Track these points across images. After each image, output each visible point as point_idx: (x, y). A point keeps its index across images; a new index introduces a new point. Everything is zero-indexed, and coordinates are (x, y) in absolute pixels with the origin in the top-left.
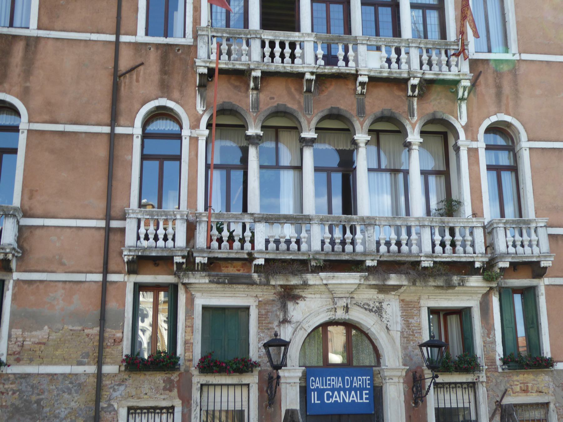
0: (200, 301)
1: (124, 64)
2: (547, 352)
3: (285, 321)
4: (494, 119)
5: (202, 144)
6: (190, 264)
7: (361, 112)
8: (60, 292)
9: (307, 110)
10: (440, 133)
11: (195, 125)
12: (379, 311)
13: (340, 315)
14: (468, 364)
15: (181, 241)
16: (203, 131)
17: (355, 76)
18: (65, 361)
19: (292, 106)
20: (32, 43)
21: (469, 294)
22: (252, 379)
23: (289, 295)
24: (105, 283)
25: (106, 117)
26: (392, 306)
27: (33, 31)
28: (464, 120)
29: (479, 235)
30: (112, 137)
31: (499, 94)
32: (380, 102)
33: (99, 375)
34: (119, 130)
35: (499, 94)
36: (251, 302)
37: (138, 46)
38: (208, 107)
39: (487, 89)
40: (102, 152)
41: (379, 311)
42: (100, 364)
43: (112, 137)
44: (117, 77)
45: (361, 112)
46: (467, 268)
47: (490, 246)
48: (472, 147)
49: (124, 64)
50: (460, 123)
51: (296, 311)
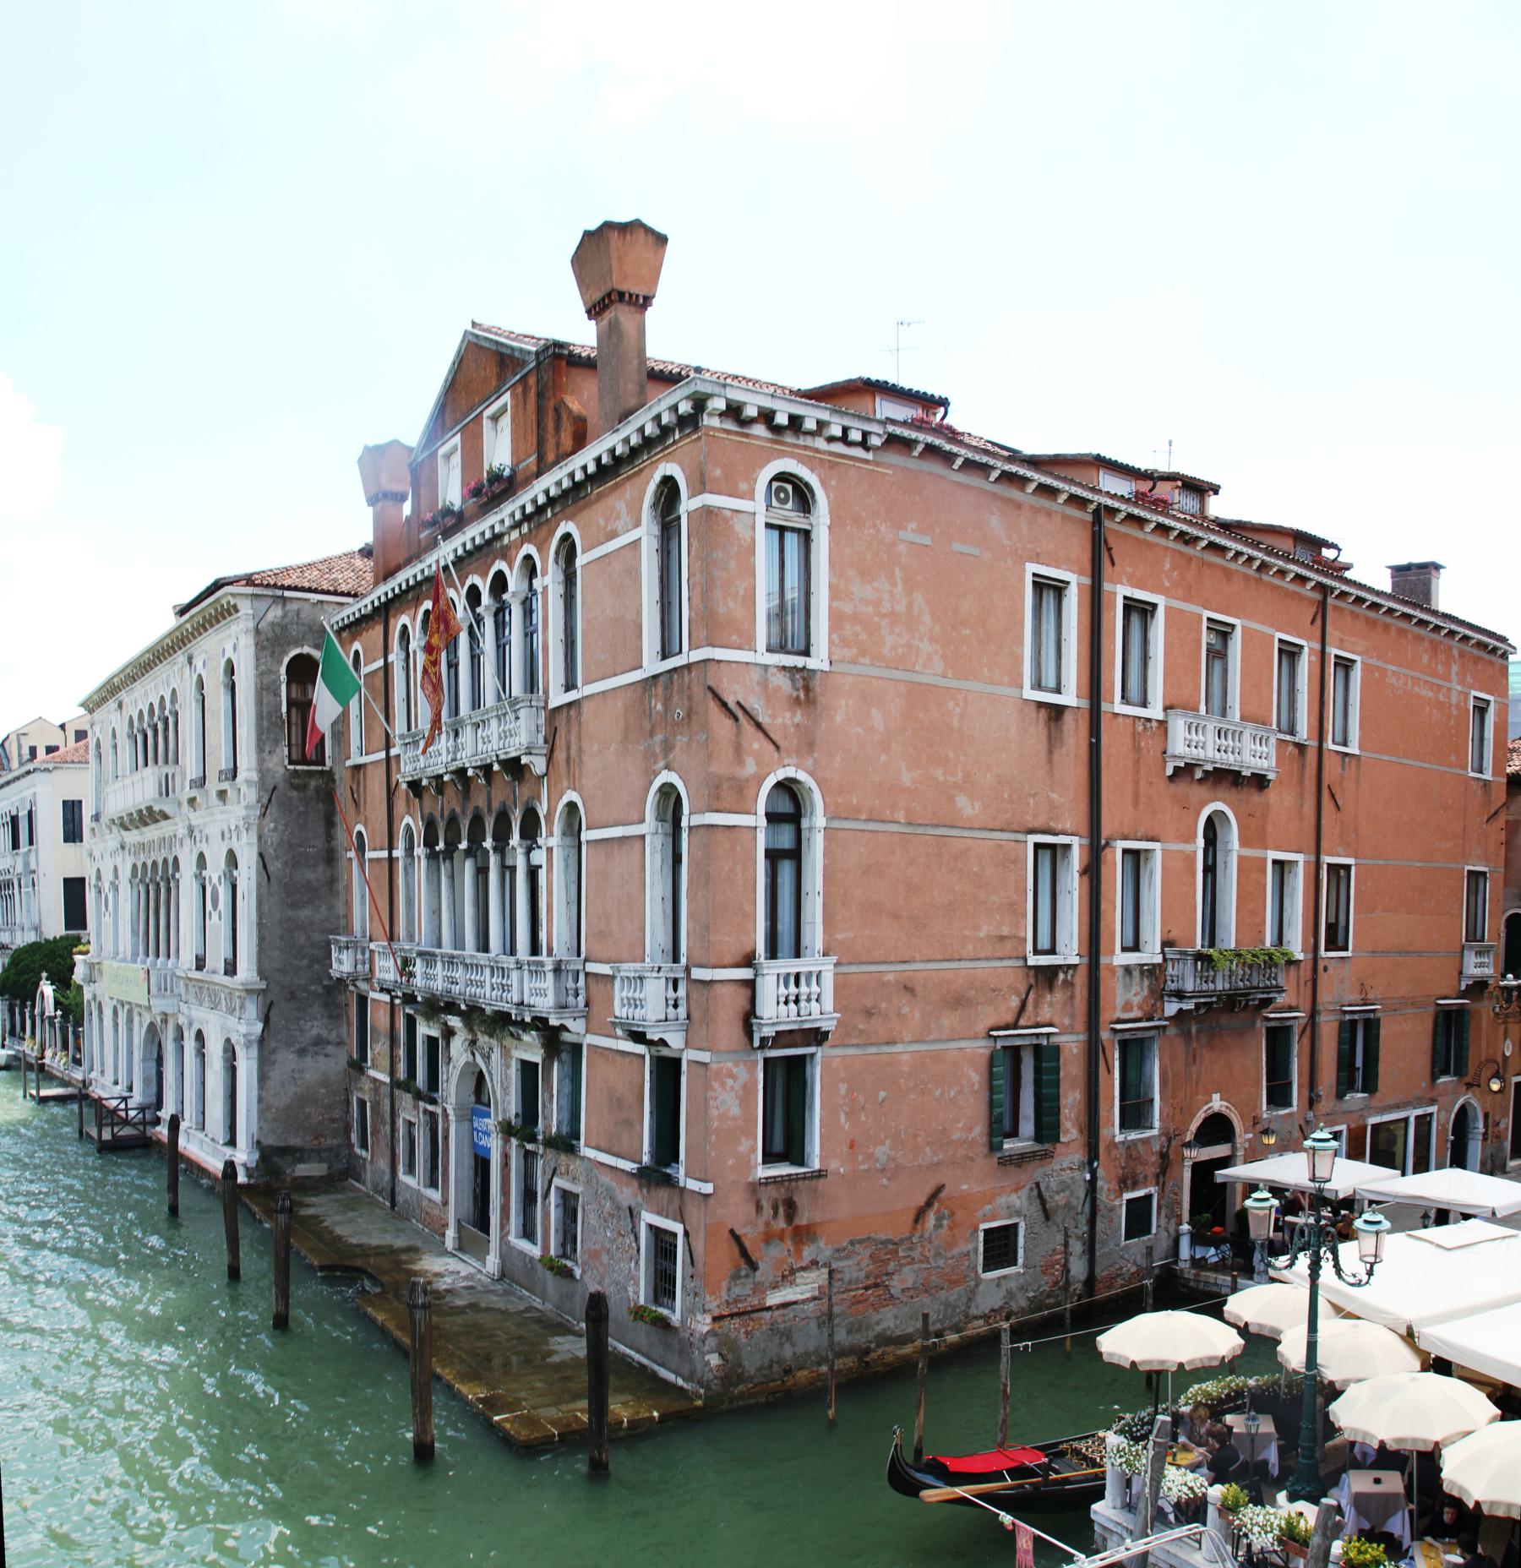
4: (565, 800)
5: (424, 862)
7: (489, 810)
8: (382, 1012)
9: (464, 813)
19: (458, 810)
34: (395, 853)
39: (560, 755)
41: (487, 1058)
50: (542, 810)
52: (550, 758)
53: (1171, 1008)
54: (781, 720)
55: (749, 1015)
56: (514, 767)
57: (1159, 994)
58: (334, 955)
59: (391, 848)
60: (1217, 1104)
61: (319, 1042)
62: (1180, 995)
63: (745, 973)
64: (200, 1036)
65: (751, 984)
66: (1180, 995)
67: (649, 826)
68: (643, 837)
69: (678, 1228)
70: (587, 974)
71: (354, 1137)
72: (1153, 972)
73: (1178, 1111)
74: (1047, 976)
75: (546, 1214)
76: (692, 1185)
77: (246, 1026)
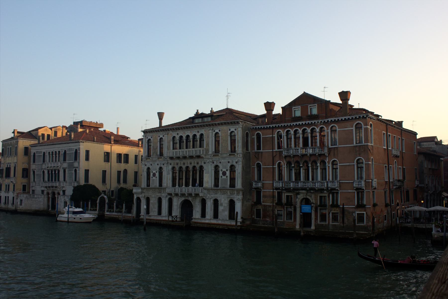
0: (286, 194)
1: (274, 155)
2: (339, 204)
3: (297, 198)
5: (286, 168)
6: (282, 190)
7: (310, 160)
10: (323, 162)
11: (284, 165)
12: (311, 197)
13: (305, 197)
14: (325, 206)
15: (281, 186)
16: (286, 166)
17: (307, 155)
18: (269, 203)
19: (299, 160)
20: (262, 152)
21: (325, 194)
22: (293, 207)
23: (298, 194)
24: (273, 191)
25: (272, 164)
26: (313, 196)
27: (261, 151)
28: (327, 160)
29: (326, 184)
30: (273, 167)
31: (334, 155)
32: (313, 158)
33: (273, 205)
35: (334, 155)
36: (293, 195)
37: (276, 151)
38: (286, 161)
40: (272, 170)
41: (311, 197)
42: (273, 203)
43: (273, 167)
44: (273, 158)
45: (310, 160)
46: (323, 189)
47: (327, 185)
48: (329, 166)
49: (274, 155)
50: (327, 161)
51: (299, 196)
52: (329, 154)
53: (395, 187)
54: (371, 151)
55: (372, 186)
56: (320, 155)
57: (393, 186)
58: (254, 184)
59: (273, 165)
60: (398, 201)
61: (249, 199)
62: (396, 185)
63: (371, 181)
64: (216, 202)
65: (372, 182)
66: (396, 185)
67: (355, 163)
68: (354, 165)
69: (365, 213)
70: (340, 183)
71: (254, 216)
72: (392, 182)
73: (396, 202)
74: (386, 182)
75: (329, 217)
76: (367, 206)
77: (240, 197)
